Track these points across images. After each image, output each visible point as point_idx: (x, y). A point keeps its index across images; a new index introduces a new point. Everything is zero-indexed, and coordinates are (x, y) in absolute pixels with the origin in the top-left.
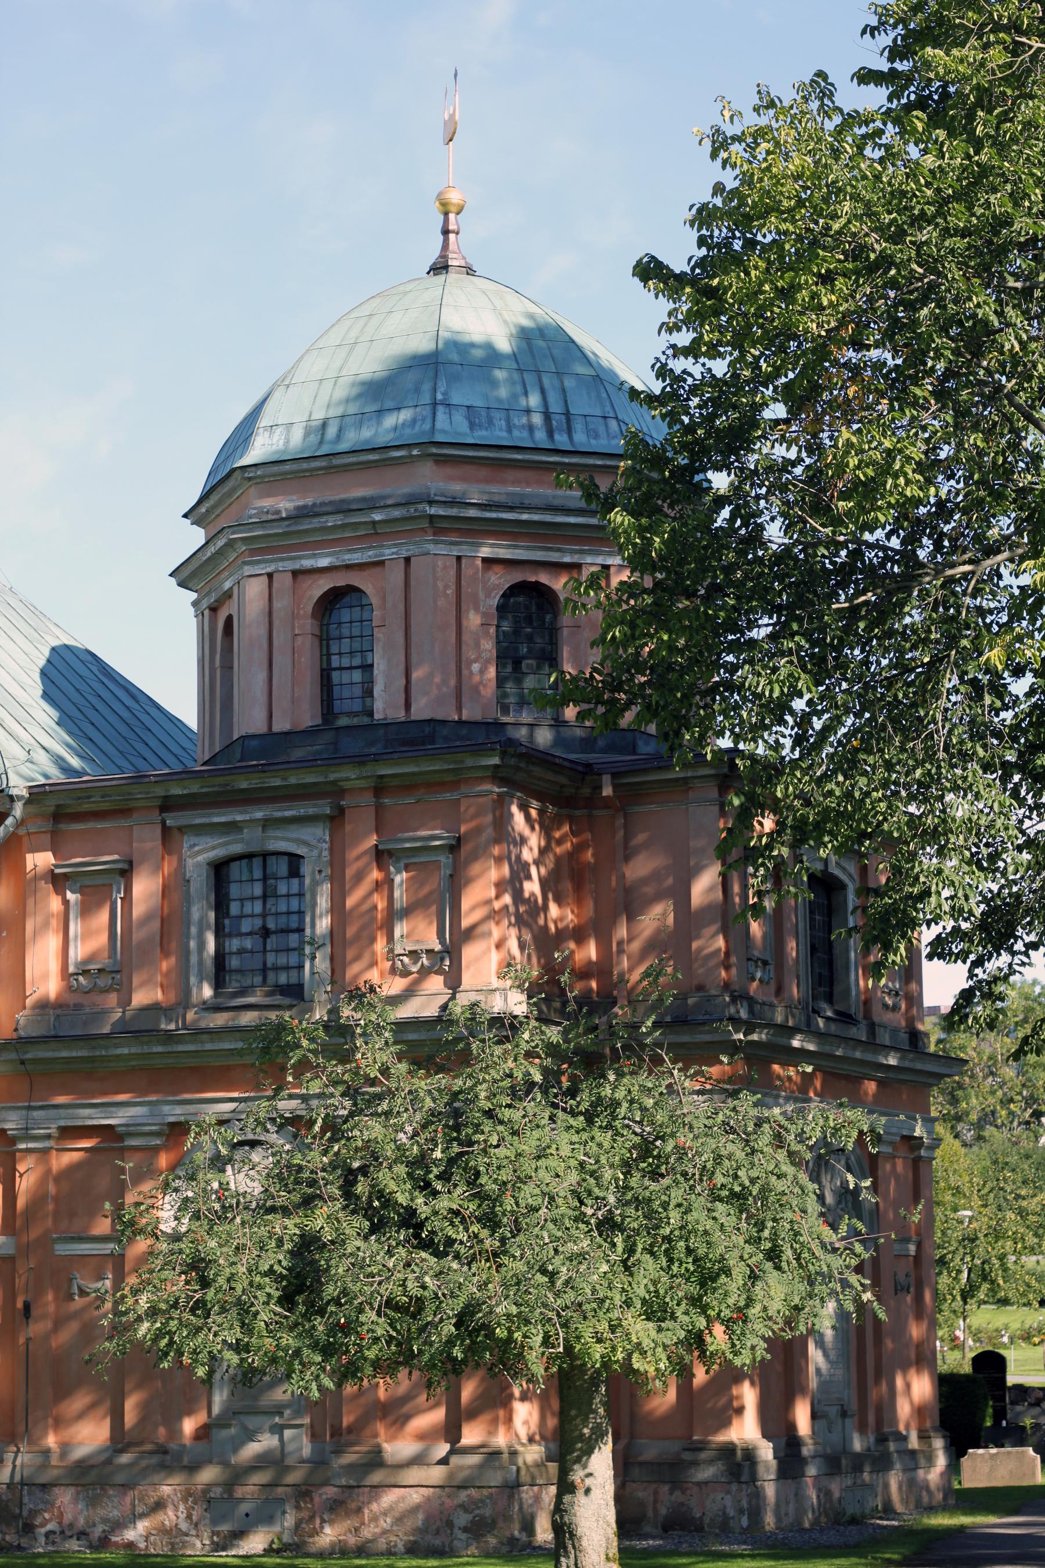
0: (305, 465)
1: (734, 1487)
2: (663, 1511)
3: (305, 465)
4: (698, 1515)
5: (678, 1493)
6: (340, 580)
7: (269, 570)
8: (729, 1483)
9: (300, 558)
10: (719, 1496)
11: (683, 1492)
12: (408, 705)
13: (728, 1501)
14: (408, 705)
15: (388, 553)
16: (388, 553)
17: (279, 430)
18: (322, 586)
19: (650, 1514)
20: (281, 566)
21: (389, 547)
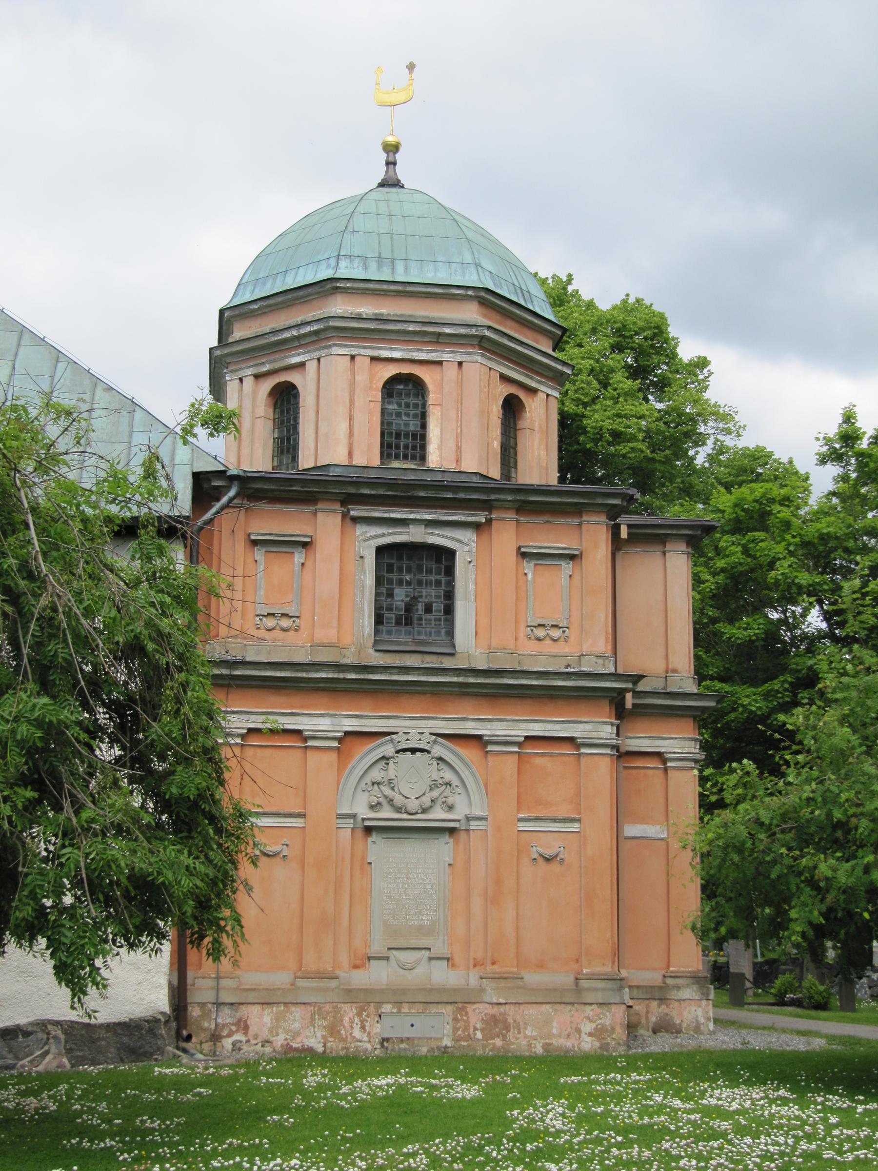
0: (385, 287)
1: (704, 1002)
2: (653, 1019)
3: (385, 287)
4: (678, 1022)
5: (664, 1006)
6: (406, 369)
7: (353, 353)
8: (701, 1000)
9: (379, 348)
10: (693, 1008)
11: (667, 1006)
12: (458, 461)
13: (700, 1012)
14: (458, 461)
15: (446, 357)
16: (446, 357)
17: (357, 260)
18: (391, 370)
19: (643, 1021)
20: (363, 352)
21: (448, 352)
